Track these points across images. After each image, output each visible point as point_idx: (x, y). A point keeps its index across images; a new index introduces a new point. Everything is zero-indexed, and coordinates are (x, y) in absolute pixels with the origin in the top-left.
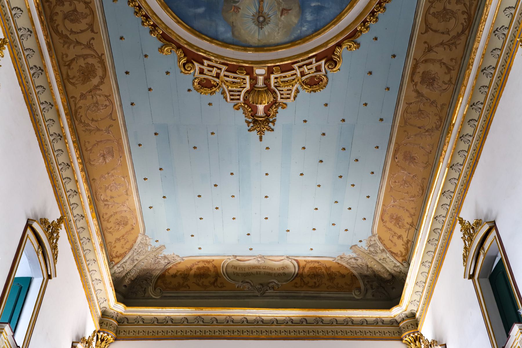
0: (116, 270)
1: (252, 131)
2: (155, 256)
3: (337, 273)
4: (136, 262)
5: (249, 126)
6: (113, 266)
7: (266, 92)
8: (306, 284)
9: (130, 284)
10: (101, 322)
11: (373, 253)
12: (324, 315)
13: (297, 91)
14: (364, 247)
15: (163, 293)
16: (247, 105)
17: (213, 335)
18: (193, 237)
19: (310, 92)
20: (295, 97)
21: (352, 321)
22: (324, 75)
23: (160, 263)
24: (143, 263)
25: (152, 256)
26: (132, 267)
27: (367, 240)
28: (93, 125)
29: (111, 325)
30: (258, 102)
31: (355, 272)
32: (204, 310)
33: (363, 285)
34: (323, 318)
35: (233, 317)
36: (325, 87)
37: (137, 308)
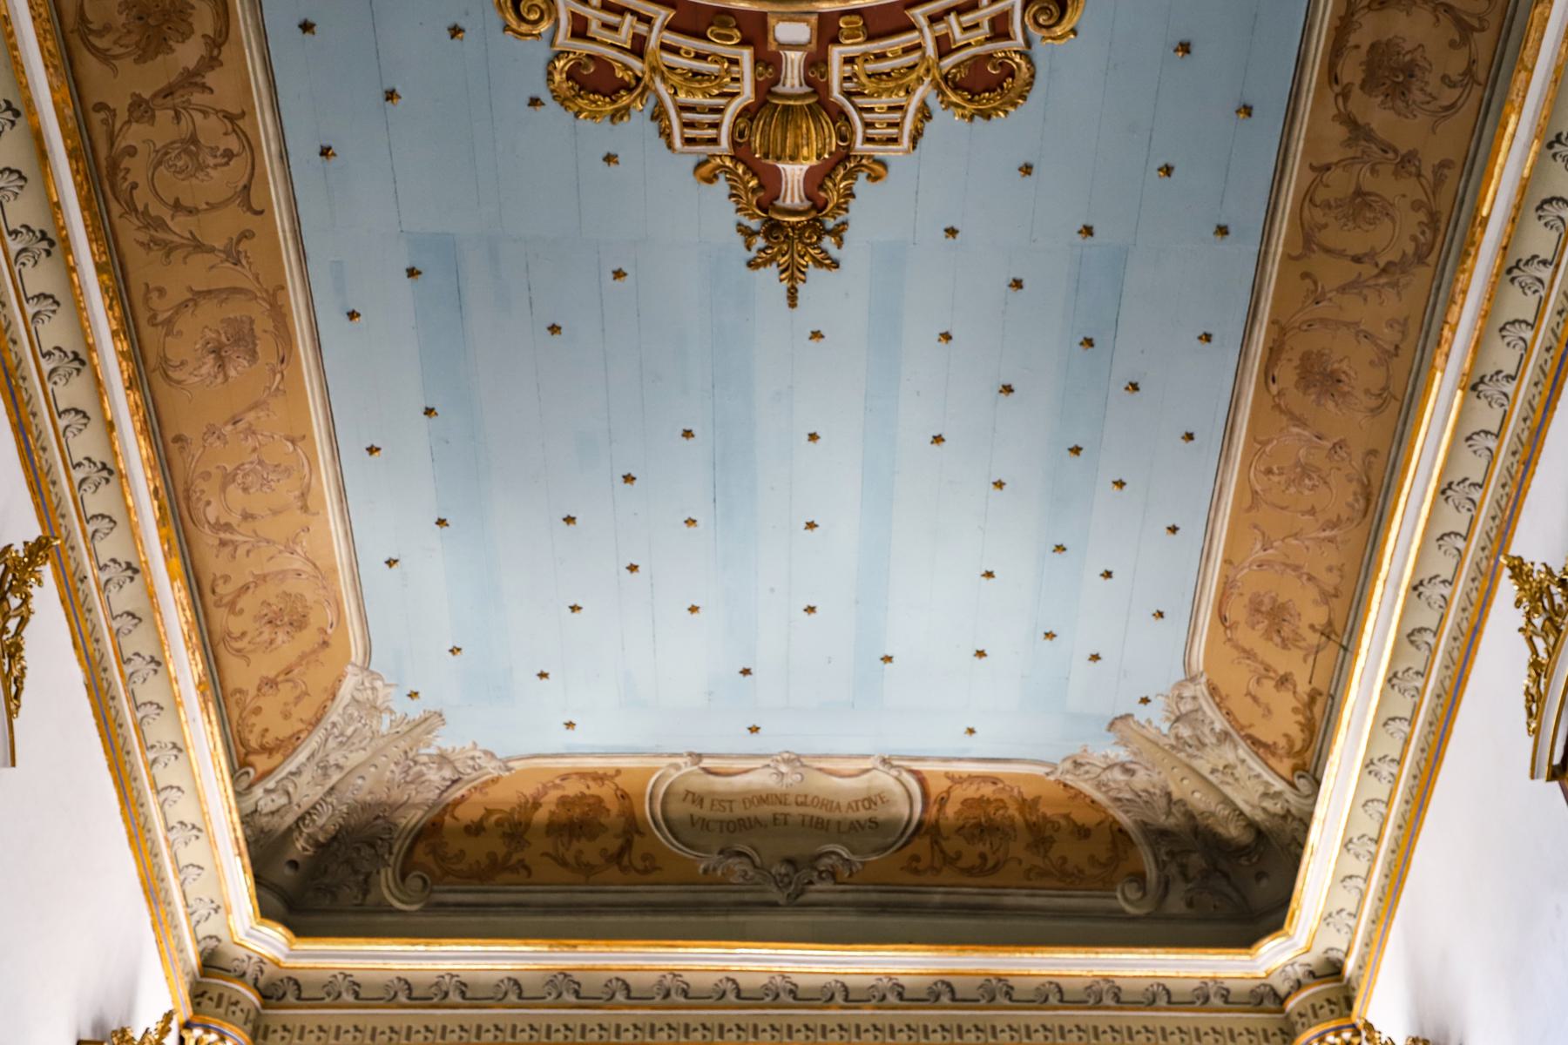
0: (261, 803)
1: (762, 269)
2: (406, 753)
3: (1063, 822)
4: (335, 777)
5: (749, 248)
6: (250, 786)
7: (813, 112)
8: (951, 860)
9: (310, 857)
10: (199, 992)
12: (1015, 970)
13: (925, 114)
14: (1156, 723)
15: (432, 891)
16: (744, 163)
17: (614, 1040)
18: (545, 680)
19: (971, 118)
20: (915, 138)
21: (1117, 994)
22: (1021, 54)
23: (423, 779)
24: (362, 777)
25: (395, 753)
26: (320, 794)
27: (1167, 697)
28: (180, 225)
29: (236, 1003)
30: (783, 149)
31: (1125, 819)
32: (580, 949)
33: (1153, 866)
34: (1012, 981)
35: (687, 977)
36: (1024, 98)
37: (333, 944)
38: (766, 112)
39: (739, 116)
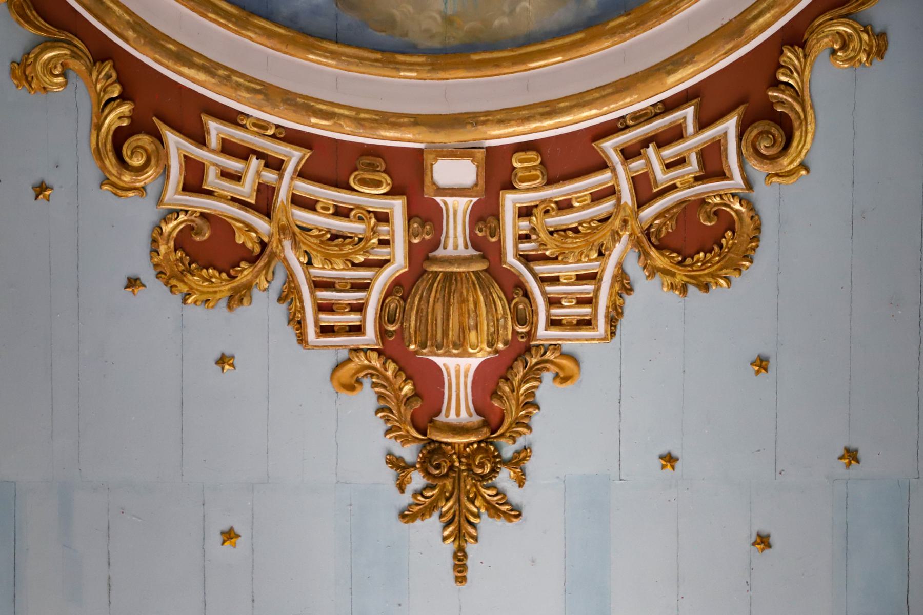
1: (418, 522)
5: (402, 489)
13: (623, 284)
19: (684, 289)
20: (613, 322)
30: (445, 333)
38: (422, 285)
39: (389, 293)
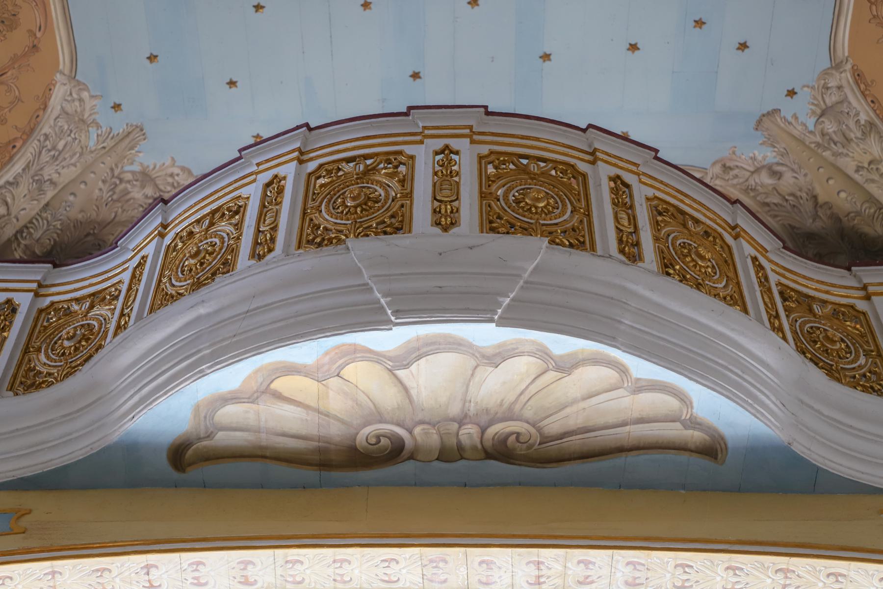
2: (112, 170)
4: (50, 194)
11: (835, 144)
14: (802, 119)
23: (128, 197)
25: (102, 169)
26: (37, 210)
27: (813, 88)
